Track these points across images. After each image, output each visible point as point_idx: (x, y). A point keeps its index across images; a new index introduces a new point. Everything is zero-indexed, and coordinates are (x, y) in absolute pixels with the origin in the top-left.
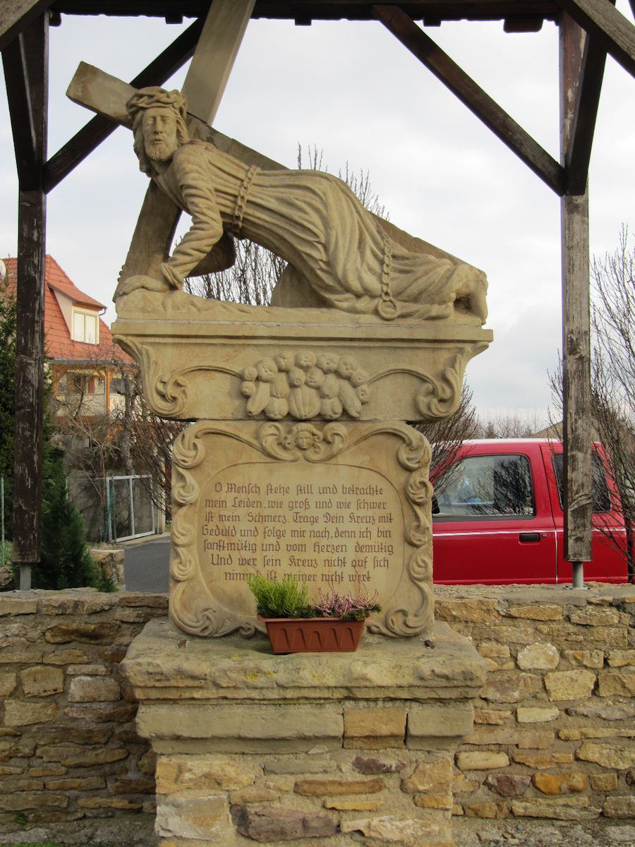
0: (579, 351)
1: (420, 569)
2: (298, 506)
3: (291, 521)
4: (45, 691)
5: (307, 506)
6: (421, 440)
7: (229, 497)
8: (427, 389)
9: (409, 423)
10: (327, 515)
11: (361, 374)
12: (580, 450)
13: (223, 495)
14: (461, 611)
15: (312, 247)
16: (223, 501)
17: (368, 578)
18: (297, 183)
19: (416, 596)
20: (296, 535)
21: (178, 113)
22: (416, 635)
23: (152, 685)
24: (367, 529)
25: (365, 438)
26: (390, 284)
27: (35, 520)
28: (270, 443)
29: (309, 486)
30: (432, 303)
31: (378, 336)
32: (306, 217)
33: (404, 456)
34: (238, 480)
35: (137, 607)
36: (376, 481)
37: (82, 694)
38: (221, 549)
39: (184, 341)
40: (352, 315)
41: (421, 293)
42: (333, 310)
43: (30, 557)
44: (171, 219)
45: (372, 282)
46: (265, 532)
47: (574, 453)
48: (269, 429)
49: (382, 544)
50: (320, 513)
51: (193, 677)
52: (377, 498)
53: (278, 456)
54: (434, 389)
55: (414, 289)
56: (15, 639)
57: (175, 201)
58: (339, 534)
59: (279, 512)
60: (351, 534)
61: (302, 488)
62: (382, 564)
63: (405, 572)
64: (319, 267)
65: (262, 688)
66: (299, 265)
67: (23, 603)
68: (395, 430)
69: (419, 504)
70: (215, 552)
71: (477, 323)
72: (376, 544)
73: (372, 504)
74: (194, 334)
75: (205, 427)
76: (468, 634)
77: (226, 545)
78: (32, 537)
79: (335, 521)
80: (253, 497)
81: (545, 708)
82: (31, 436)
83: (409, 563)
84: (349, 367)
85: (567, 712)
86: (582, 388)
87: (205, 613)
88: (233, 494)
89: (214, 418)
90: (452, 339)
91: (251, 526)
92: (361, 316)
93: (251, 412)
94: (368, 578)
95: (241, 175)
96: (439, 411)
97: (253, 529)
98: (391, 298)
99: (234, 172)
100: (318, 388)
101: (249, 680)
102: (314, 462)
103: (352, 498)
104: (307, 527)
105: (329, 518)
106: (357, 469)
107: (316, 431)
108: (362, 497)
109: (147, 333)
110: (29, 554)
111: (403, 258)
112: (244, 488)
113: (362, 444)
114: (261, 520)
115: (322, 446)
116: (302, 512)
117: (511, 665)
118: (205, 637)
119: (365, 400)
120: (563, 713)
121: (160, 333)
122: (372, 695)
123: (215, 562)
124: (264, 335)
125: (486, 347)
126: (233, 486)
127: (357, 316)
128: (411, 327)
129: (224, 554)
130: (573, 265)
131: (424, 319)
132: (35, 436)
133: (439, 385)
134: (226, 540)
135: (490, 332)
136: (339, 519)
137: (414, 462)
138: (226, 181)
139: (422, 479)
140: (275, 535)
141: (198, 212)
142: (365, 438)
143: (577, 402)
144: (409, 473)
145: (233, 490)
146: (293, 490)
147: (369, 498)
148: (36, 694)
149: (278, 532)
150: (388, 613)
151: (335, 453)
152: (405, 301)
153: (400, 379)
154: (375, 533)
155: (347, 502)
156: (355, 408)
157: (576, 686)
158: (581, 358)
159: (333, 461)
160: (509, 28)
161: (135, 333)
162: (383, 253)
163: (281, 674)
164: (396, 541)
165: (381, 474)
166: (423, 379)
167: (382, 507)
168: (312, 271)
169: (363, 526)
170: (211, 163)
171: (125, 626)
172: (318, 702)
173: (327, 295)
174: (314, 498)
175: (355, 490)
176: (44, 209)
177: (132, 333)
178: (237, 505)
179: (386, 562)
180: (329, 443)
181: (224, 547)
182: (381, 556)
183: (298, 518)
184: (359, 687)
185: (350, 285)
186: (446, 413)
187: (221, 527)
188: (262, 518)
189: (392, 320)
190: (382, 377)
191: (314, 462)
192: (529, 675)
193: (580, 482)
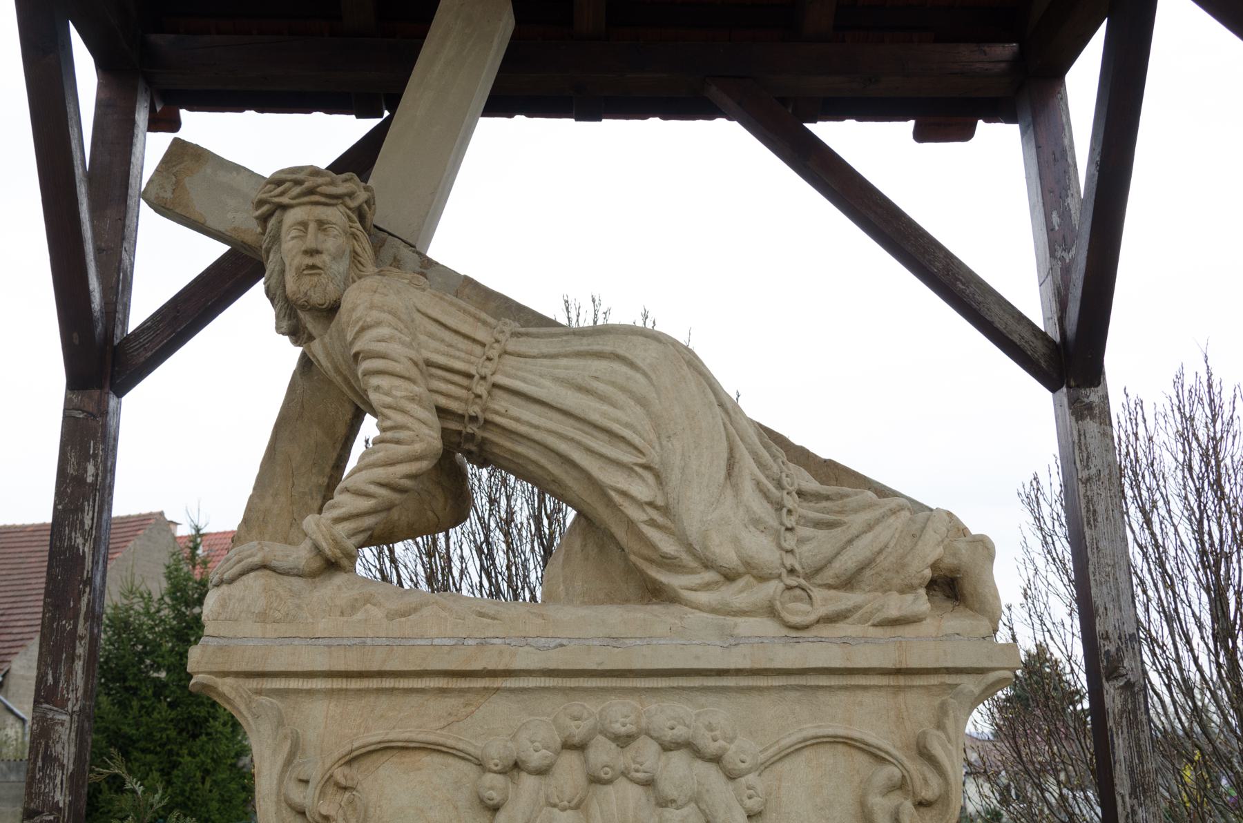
0: (1124, 672)
8: (889, 779)
11: (743, 750)
18: (596, 348)
21: (355, 218)
26: (797, 551)
30: (885, 588)
32: (618, 414)
39: (355, 684)
40: (720, 619)
41: (861, 569)
42: (675, 609)
44: (341, 429)
45: (762, 548)
54: (903, 776)
55: (848, 561)
57: (345, 389)
64: (645, 518)
66: (602, 513)
74: (375, 668)
84: (717, 733)
86: (1138, 745)
92: (740, 620)
95: (481, 334)
98: (803, 582)
99: (465, 329)
100: (649, 783)
111: (818, 497)
119: (757, 808)
121: (299, 669)
124: (532, 667)
127: (731, 620)
128: (845, 642)
130: (1095, 511)
131: (874, 625)
133: (916, 768)
138: (450, 346)
141: (389, 407)
152: (830, 587)
153: (828, 757)
158: (1129, 686)
160: (921, 135)
161: (244, 667)
162: (780, 485)
166: (878, 757)
168: (630, 524)
170: (419, 311)
173: (663, 577)
176: (112, 423)
177: (234, 669)
185: (714, 553)
189: (806, 627)
190: (787, 755)
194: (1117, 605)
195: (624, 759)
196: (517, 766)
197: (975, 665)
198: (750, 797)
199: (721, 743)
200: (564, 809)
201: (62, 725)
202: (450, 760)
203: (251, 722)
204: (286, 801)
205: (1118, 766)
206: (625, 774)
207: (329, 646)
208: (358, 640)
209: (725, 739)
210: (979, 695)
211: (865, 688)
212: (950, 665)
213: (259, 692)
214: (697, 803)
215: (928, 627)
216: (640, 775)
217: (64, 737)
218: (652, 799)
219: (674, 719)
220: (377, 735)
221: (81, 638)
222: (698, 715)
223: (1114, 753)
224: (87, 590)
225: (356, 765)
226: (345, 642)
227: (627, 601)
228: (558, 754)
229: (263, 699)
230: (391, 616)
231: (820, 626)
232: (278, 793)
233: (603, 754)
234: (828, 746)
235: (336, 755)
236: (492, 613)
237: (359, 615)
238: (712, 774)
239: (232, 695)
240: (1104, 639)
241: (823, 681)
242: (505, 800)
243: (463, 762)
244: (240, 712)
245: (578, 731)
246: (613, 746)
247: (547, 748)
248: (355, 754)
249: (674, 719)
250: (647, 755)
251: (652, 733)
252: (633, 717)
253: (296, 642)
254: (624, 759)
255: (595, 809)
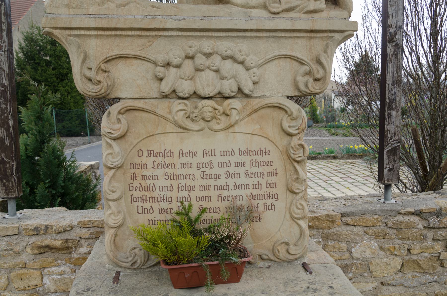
0: (395, 40)
1: (299, 211)
2: (204, 166)
4: (29, 286)
6: (300, 111)
7: (149, 161)
8: (305, 71)
11: (251, 60)
12: (393, 109)
13: (144, 159)
14: (315, 222)
16: (144, 164)
17: (260, 219)
20: (203, 189)
22: (296, 259)
24: (258, 182)
25: (256, 111)
27: (14, 168)
28: (180, 117)
33: (286, 125)
34: (156, 148)
35: (90, 227)
36: (265, 144)
37: (55, 287)
38: (144, 201)
39: (106, 33)
40: (245, 10)
42: (228, 6)
43: (13, 193)
46: (179, 188)
47: (390, 112)
48: (177, 105)
49: (269, 193)
50: (222, 171)
52: (266, 158)
53: (188, 127)
54: (310, 70)
56: (5, 252)
58: (237, 187)
60: (246, 186)
61: (207, 152)
62: (270, 208)
67: (8, 228)
69: (298, 162)
70: (140, 204)
72: (266, 194)
73: (262, 163)
74: (113, 26)
76: (319, 237)
77: (148, 199)
78: (13, 180)
79: (233, 177)
80: (168, 160)
81: (369, 283)
82: (6, 108)
84: (243, 53)
85: (382, 284)
86: (397, 67)
87: (133, 251)
88: (152, 159)
89: (134, 97)
91: (168, 183)
92: (252, 10)
93: (164, 92)
96: (314, 88)
100: (217, 71)
102: (216, 131)
103: (247, 159)
104: (212, 182)
105: (229, 175)
106: (250, 135)
107: (217, 106)
108: (254, 158)
110: (12, 192)
112: (161, 154)
113: (254, 116)
114: (175, 178)
115: (223, 118)
116: (208, 171)
117: (347, 255)
118: (135, 269)
120: (380, 285)
121: (84, 26)
123: (140, 212)
124: (173, 27)
126: (152, 152)
127: (249, 10)
128: (292, 19)
129: (147, 205)
131: (304, 13)
132: (9, 108)
133: (315, 67)
134: (148, 194)
136: (237, 176)
139: (300, 142)
140: (187, 189)
142: (256, 111)
143: (393, 76)
144: (289, 137)
145: (152, 155)
146: (200, 154)
147: (259, 158)
148: (23, 288)
149: (189, 187)
150: (275, 244)
151: (232, 124)
153: (283, 63)
154: (264, 185)
156: (247, 89)
157: (389, 268)
158: (397, 45)
159: (231, 130)
164: (280, 190)
165: (269, 139)
166: (301, 63)
167: (269, 164)
169: (255, 180)
171: (83, 241)
174: (216, 160)
175: (248, 152)
177: (59, 26)
178: (156, 167)
179: (273, 206)
180: (227, 115)
181: (146, 200)
182: (269, 202)
183: (205, 176)
186: (320, 89)
187: (143, 185)
188: (175, 177)
189: (278, 13)
190: (268, 62)
191: (216, 131)
192: (359, 262)
193: (393, 132)
194: (397, 14)
195: (208, 62)
196: (168, 65)
197: (341, 29)
198: (254, 77)
199: (244, 57)
200: (186, 80)
201: (2, 55)
202: (144, 62)
203: (68, 47)
204: (84, 76)
205: (388, 74)
206: (208, 68)
207: (95, 18)
208: (106, 16)
209: (246, 55)
210: (341, 40)
211: (298, 37)
212: (331, 29)
213: (70, 35)
214: (235, 78)
215: (324, 14)
216: (214, 68)
217: (3, 60)
218: (218, 77)
219: (227, 48)
220: (116, 52)
221: (4, 23)
222: (236, 47)
223: (388, 70)
224: (3, 4)
225: (109, 63)
226: (101, 16)
227: (210, 4)
228: (184, 60)
229: (72, 38)
230: (118, 6)
231: (283, 13)
232: (81, 73)
233: (200, 60)
234: (283, 59)
235: (101, 59)
236: (157, 6)
237: (106, 6)
238: (240, 68)
239: (60, 36)
240: (390, 27)
241: (283, 34)
242: (165, 76)
243: (149, 63)
244: (64, 43)
245: (191, 52)
246: (204, 57)
247: (179, 58)
248: (108, 59)
249: (227, 48)
250: (216, 61)
251: (219, 53)
252: (211, 47)
253: (82, 16)
254: (208, 62)
255: (197, 80)
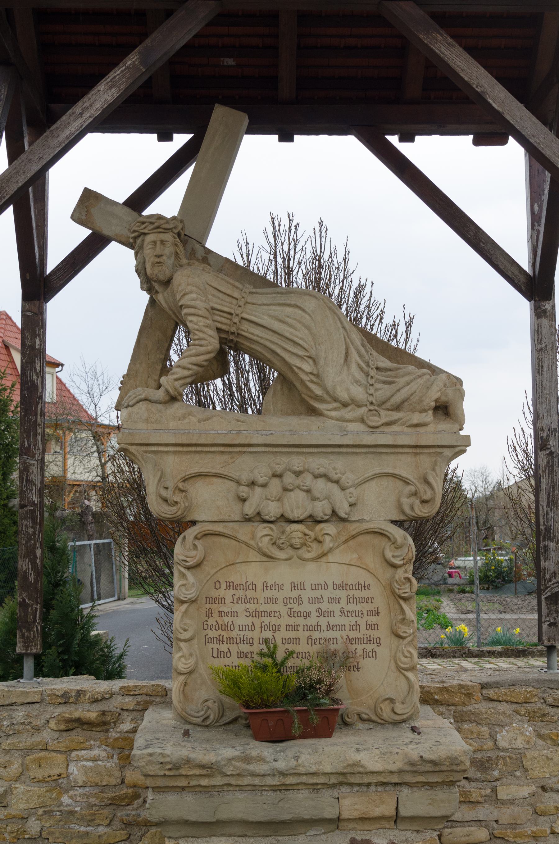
0: (549, 447)
1: (406, 660)
2: (292, 601)
3: (286, 616)
4: (50, 776)
5: (301, 602)
6: (405, 538)
7: (228, 595)
9: (393, 522)
10: (319, 610)
11: (348, 478)
12: (551, 540)
13: (222, 592)
14: (443, 695)
15: (302, 361)
16: (221, 598)
17: (358, 668)
18: (288, 302)
19: (404, 684)
20: (290, 629)
21: (176, 236)
22: (404, 721)
23: (162, 774)
24: (356, 622)
25: (354, 537)
26: (374, 394)
27: (38, 612)
28: (265, 543)
29: (302, 584)
30: (413, 411)
31: (364, 443)
32: (297, 333)
33: (389, 554)
34: (236, 579)
35: (136, 695)
36: (364, 577)
37: (84, 779)
38: (221, 643)
39: (185, 449)
40: (340, 423)
41: (403, 402)
42: (321, 418)
43: (33, 648)
44: (170, 333)
45: (359, 393)
46: (261, 627)
47: (546, 543)
48: (262, 530)
49: (370, 636)
50: (312, 608)
51: (203, 767)
52: (365, 594)
53: (273, 556)
54: (416, 490)
55: (397, 399)
56: (21, 726)
57: (173, 316)
58: (330, 627)
59: (275, 607)
60: (342, 627)
61: (296, 585)
62: (371, 655)
63: (392, 662)
64: (309, 379)
65: (264, 775)
66: (290, 375)
67: (28, 693)
68: (381, 529)
69: (404, 599)
70: (215, 646)
71: (455, 430)
72: (365, 637)
73: (361, 599)
74: (194, 442)
75: (204, 529)
76: (450, 717)
77: (225, 639)
78: (35, 629)
79: (326, 615)
80: (250, 594)
81: (523, 786)
82: (34, 533)
83: (395, 656)
84: (338, 471)
85: (543, 788)
87: (205, 704)
88: (232, 592)
89: (213, 520)
90: (434, 444)
91: (249, 621)
92: (348, 424)
93: (247, 515)
94: (358, 668)
95: (236, 294)
96: (421, 511)
97: (250, 624)
98: (376, 408)
99: (228, 292)
100: (308, 491)
101: (251, 767)
102: (306, 560)
103: (342, 594)
104: (301, 621)
105: (321, 613)
106: (346, 566)
107: (307, 531)
108: (351, 593)
109: (150, 442)
110: (32, 645)
111: (386, 370)
112: (242, 586)
113: (351, 543)
114: (257, 616)
115: (314, 545)
116: (296, 608)
117: (490, 744)
118: (207, 726)
119: (353, 502)
120: (540, 790)
122: (366, 780)
123: (215, 655)
124: (260, 443)
125: (465, 451)
126: (231, 584)
127: (345, 424)
128: (394, 434)
129: (224, 647)
130: (542, 366)
131: (407, 427)
132: (37, 533)
133: (422, 487)
134: (225, 634)
135: (468, 437)
136: (331, 614)
137: (399, 559)
138: (222, 300)
139: (406, 575)
140: (271, 629)
141: (197, 330)
142: (354, 537)
143: (548, 495)
144: (393, 569)
145: (231, 587)
146: (287, 587)
147: (358, 594)
148: (41, 778)
149: (274, 626)
150: (376, 702)
151: (325, 552)
152: (389, 410)
153: (385, 482)
154: (363, 627)
155: (337, 597)
156: (343, 510)
157: (551, 764)
159: (324, 559)
160: (476, 143)
161: (140, 442)
162: (368, 366)
163: (279, 762)
164: (383, 633)
165: (369, 571)
166: (406, 482)
167: (370, 601)
168: (302, 382)
169: (353, 620)
170: (208, 284)
171: (125, 714)
172: (316, 787)
173: (317, 405)
174: (307, 594)
175: (344, 586)
176: (44, 317)
177: (136, 442)
178: (235, 601)
179: (374, 653)
180: (320, 542)
181: (223, 641)
182: (369, 647)
183: (292, 613)
184: (353, 773)
185: (338, 395)
186: (428, 513)
187: (220, 623)
188: (258, 614)
190: (368, 481)
191: (306, 560)
192: (508, 754)
193: (552, 571)
194: (549, 414)
195: (298, 481)
196: (253, 484)
197: (450, 444)
198: (351, 497)
199: (339, 475)
200: (273, 501)
201: (34, 466)
202: (225, 481)
203: (144, 464)
204: (159, 496)
205: (542, 492)
206: (298, 487)
207: (175, 433)
208: (186, 431)
209: (341, 474)
210: (452, 457)
211: (402, 453)
212: (439, 444)
213: (146, 452)
214: (328, 500)
215: (431, 428)
216: (305, 488)
217: (35, 471)
218: (310, 498)
219: (319, 465)
220: (195, 470)
221: (39, 425)
222: (330, 464)
223: (540, 486)
224: (40, 401)
225: (186, 482)
226: (181, 432)
227: (301, 414)
228: (270, 478)
229: (148, 455)
230: (200, 421)
231: (384, 427)
232: (156, 492)
233: (289, 479)
234: (385, 477)
235: (179, 478)
236: (242, 420)
237: (186, 420)
238: (335, 489)
239: (136, 453)
240: (541, 431)
241: (384, 450)
242: (249, 497)
243: (231, 482)
244: (139, 460)
245: (279, 469)
246: (294, 476)
247: (266, 476)
248: (187, 477)
249: (319, 465)
250: (308, 479)
251: (310, 471)
252: (302, 464)
253: (161, 431)
254: (298, 481)
255: (286, 501)
